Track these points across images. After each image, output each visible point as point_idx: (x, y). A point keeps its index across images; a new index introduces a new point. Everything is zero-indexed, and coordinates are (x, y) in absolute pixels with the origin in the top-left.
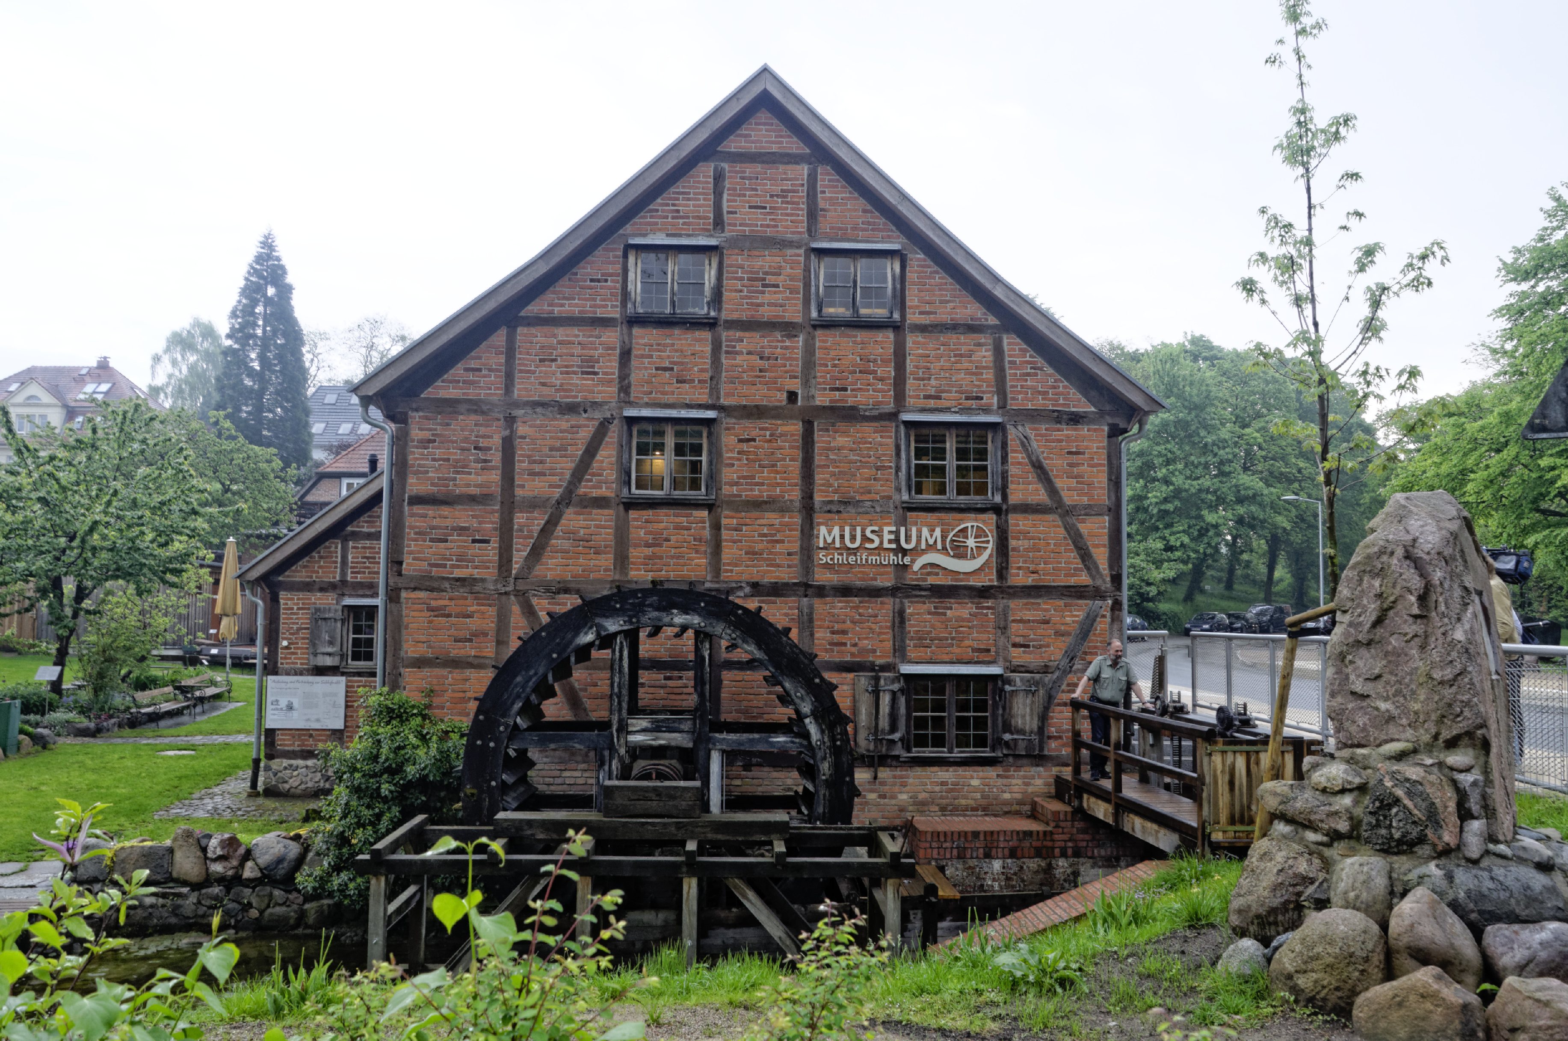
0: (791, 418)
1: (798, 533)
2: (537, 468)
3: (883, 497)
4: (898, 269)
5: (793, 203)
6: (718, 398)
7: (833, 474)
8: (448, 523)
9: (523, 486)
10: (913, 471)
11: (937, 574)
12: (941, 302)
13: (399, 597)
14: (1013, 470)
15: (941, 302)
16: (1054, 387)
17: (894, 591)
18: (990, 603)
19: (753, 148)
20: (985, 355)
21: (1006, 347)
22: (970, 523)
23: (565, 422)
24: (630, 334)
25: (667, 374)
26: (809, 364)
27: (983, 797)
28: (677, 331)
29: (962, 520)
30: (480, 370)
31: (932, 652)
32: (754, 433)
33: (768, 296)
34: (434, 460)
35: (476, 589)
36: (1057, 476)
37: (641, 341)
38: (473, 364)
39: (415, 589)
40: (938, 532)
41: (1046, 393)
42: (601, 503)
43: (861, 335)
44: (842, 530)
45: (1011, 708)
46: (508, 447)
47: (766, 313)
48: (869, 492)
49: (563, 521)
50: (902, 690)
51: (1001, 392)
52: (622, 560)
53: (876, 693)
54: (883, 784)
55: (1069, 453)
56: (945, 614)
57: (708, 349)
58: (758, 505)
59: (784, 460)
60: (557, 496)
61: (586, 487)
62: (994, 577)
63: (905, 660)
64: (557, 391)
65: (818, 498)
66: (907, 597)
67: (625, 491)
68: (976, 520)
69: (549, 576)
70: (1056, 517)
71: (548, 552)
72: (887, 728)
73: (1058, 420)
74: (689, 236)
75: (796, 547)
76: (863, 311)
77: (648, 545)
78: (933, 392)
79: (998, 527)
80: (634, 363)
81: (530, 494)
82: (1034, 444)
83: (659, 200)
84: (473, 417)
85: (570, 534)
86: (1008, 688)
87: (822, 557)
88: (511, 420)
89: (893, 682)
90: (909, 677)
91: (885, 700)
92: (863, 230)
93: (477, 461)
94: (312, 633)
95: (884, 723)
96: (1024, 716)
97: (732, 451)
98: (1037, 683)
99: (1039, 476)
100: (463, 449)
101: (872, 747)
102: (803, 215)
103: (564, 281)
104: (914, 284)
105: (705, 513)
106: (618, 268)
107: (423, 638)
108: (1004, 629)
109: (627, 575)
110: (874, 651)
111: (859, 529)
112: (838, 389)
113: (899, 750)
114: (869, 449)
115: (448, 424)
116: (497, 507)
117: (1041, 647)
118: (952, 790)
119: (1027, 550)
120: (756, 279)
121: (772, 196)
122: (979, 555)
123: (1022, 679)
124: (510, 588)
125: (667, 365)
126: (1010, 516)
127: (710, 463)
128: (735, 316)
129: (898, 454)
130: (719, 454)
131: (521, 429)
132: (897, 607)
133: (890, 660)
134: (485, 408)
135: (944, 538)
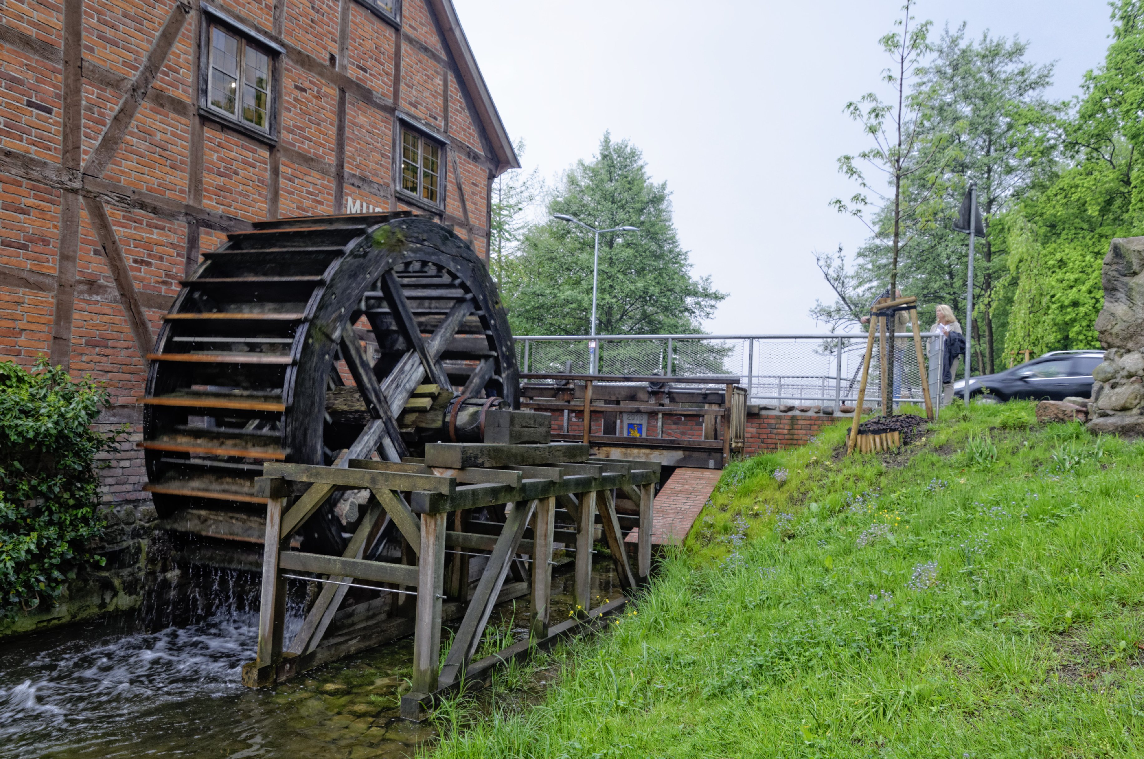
0: (332, 81)
1: (332, 198)
2: (109, 33)
7: (356, 148)
35: (35, 174)
59: (325, 121)
71: (121, 150)
77: (220, 175)
85: (146, 133)
97: (290, 95)
105: (266, 154)
109: (200, 202)
116: (60, 67)
124: (77, 185)
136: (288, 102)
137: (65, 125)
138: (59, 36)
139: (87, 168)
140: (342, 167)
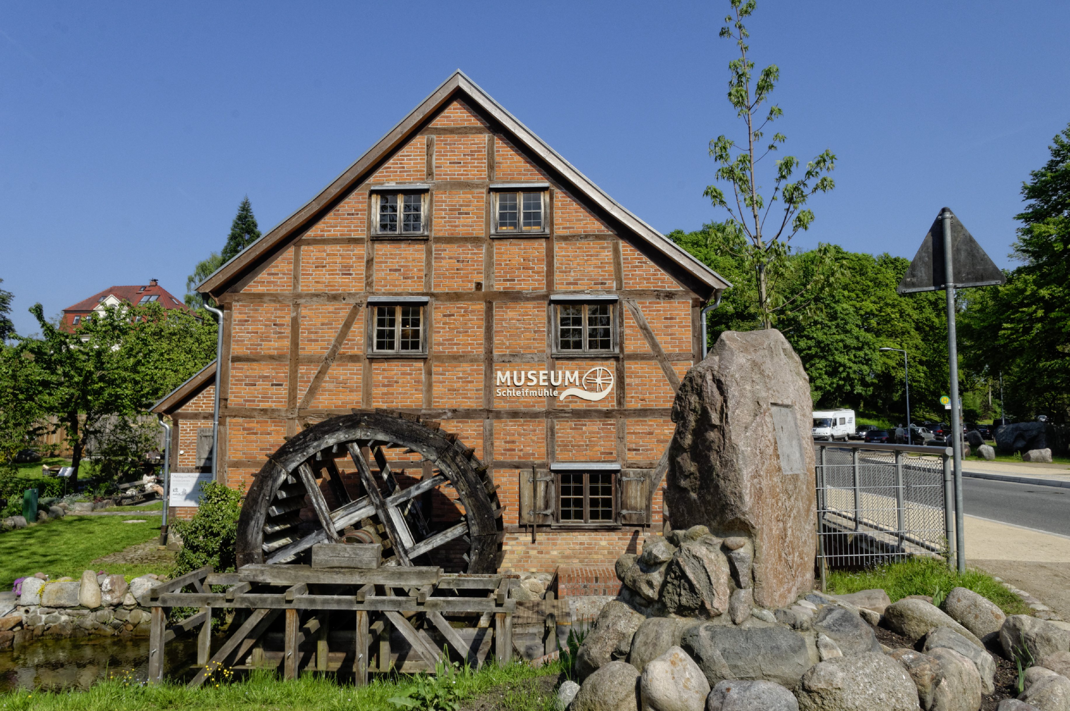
0: (479, 300)
2: (313, 337)
3: (539, 351)
4: (548, 199)
5: (478, 159)
6: (430, 288)
7: (506, 336)
8: (256, 373)
9: (304, 349)
10: (559, 334)
11: (576, 402)
12: (577, 220)
13: (225, 422)
14: (627, 331)
15: (577, 220)
16: (655, 275)
17: (548, 414)
18: (612, 421)
19: (452, 125)
20: (607, 255)
21: (621, 249)
22: (599, 367)
23: (331, 307)
24: (373, 248)
25: (397, 274)
26: (490, 264)
27: (609, 553)
28: (403, 245)
29: (593, 366)
30: (277, 274)
31: (573, 455)
32: (454, 311)
33: (463, 220)
34: (248, 333)
36: (657, 335)
37: (380, 253)
38: (273, 270)
39: (235, 416)
40: (576, 374)
41: (649, 279)
42: (354, 359)
43: (523, 244)
44: (512, 373)
45: (627, 492)
46: (295, 323)
47: (461, 231)
48: (530, 348)
49: (330, 371)
50: (553, 481)
51: (619, 280)
52: (368, 396)
53: (535, 483)
54: (540, 544)
55: (666, 318)
56: (582, 429)
57: (424, 256)
58: (456, 358)
59: (473, 328)
60: (326, 354)
61: (344, 348)
62: (615, 404)
63: (554, 459)
64: (326, 286)
65: (496, 353)
66: (557, 417)
67: (370, 350)
68: (602, 365)
69: (321, 407)
70: (658, 362)
71: (320, 391)
72: (543, 506)
73: (658, 297)
74: (410, 183)
75: (482, 386)
76: (524, 228)
77: (384, 386)
78: (571, 280)
79: (617, 369)
80: (375, 267)
81: (309, 354)
82: (641, 313)
83: (391, 161)
84: (273, 304)
85: (335, 379)
86: (624, 479)
87: (499, 392)
88: (297, 305)
89: (546, 475)
90: (556, 472)
91: (541, 488)
92: (525, 175)
93: (275, 333)
94: (198, 446)
95: (540, 503)
96: (636, 498)
98: (644, 475)
99: (645, 335)
100: (266, 325)
101: (532, 519)
102: (485, 166)
103: (331, 214)
104: (559, 209)
105: (421, 364)
106: (365, 206)
107: (240, 448)
108: (621, 439)
110: (534, 454)
111: (523, 373)
112: (508, 280)
113: (550, 521)
114: (530, 319)
115: (257, 310)
116: (288, 363)
117: (647, 450)
118: (588, 548)
119: (637, 385)
120: (455, 210)
121: (464, 155)
122: (605, 389)
123: (634, 473)
125: (397, 268)
126: (625, 362)
127: (425, 331)
128: (441, 234)
129: (549, 322)
130: (431, 326)
131: (303, 311)
132: (549, 424)
133: (545, 460)
134: (280, 299)
135: (580, 378)
136: (438, 328)
137: (290, 389)
138: (288, 349)
139: (300, 406)
140: (491, 352)
